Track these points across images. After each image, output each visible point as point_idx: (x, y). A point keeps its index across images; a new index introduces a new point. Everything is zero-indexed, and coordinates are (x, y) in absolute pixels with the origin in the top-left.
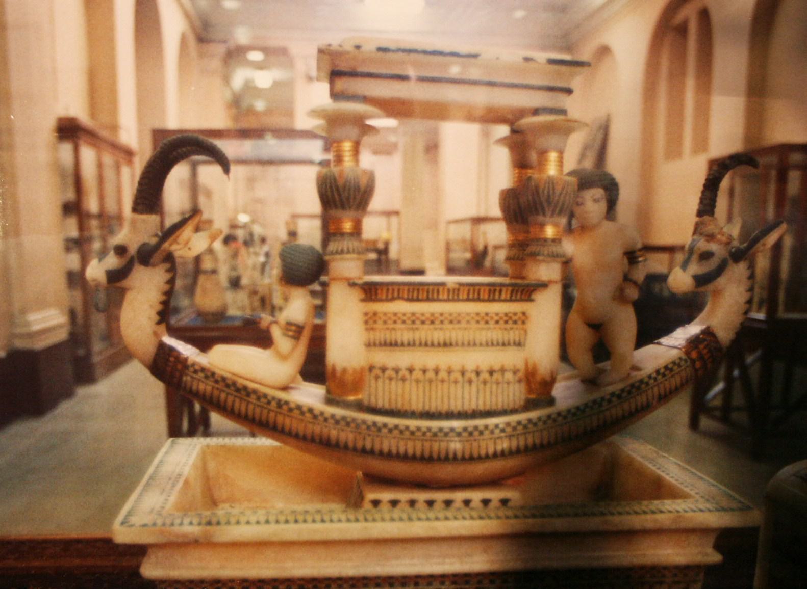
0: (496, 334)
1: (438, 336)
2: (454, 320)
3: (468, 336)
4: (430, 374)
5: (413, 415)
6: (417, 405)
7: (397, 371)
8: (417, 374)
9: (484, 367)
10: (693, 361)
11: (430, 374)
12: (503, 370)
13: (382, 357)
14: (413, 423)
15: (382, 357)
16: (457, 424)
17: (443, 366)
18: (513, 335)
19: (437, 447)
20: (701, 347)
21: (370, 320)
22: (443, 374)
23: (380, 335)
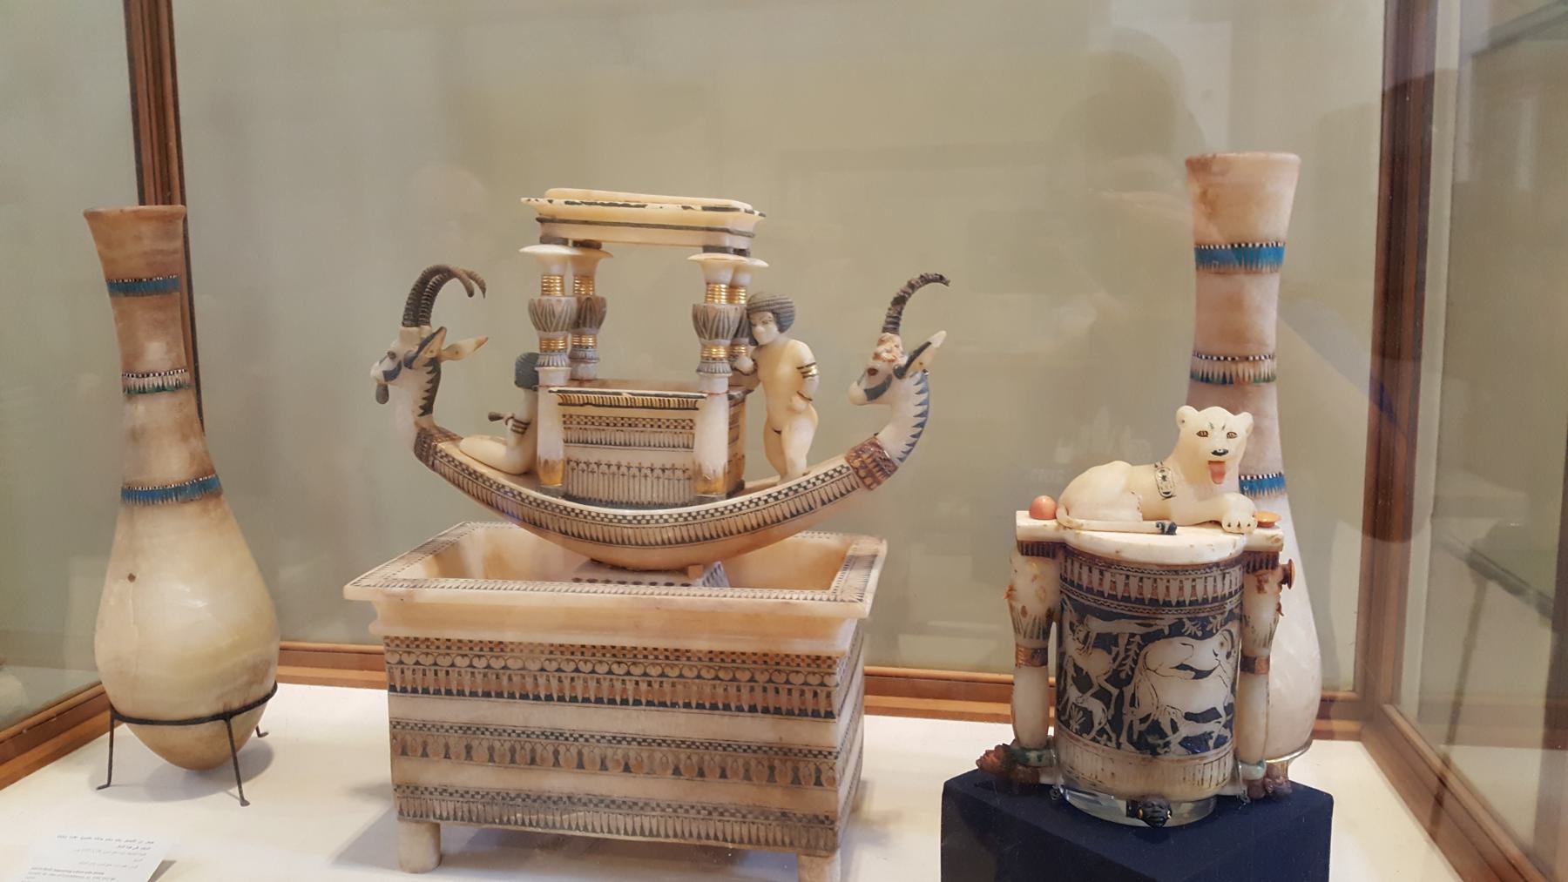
0: (666, 437)
1: (620, 437)
2: (632, 424)
3: (644, 438)
4: (614, 468)
5: (600, 503)
6: (603, 495)
7: (587, 464)
8: (604, 468)
9: (657, 465)
10: (857, 470)
11: (614, 468)
12: (673, 469)
13: (579, 453)
14: (594, 509)
15: (579, 453)
16: (628, 512)
17: (635, 464)
18: (680, 439)
19: (613, 532)
20: (865, 456)
21: (567, 421)
22: (623, 469)
23: (575, 436)
